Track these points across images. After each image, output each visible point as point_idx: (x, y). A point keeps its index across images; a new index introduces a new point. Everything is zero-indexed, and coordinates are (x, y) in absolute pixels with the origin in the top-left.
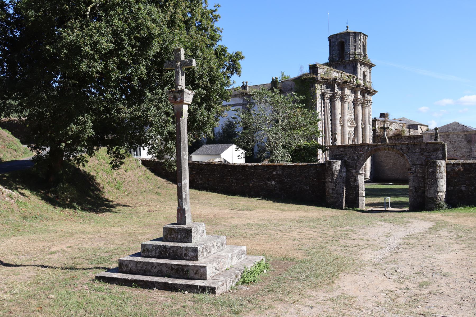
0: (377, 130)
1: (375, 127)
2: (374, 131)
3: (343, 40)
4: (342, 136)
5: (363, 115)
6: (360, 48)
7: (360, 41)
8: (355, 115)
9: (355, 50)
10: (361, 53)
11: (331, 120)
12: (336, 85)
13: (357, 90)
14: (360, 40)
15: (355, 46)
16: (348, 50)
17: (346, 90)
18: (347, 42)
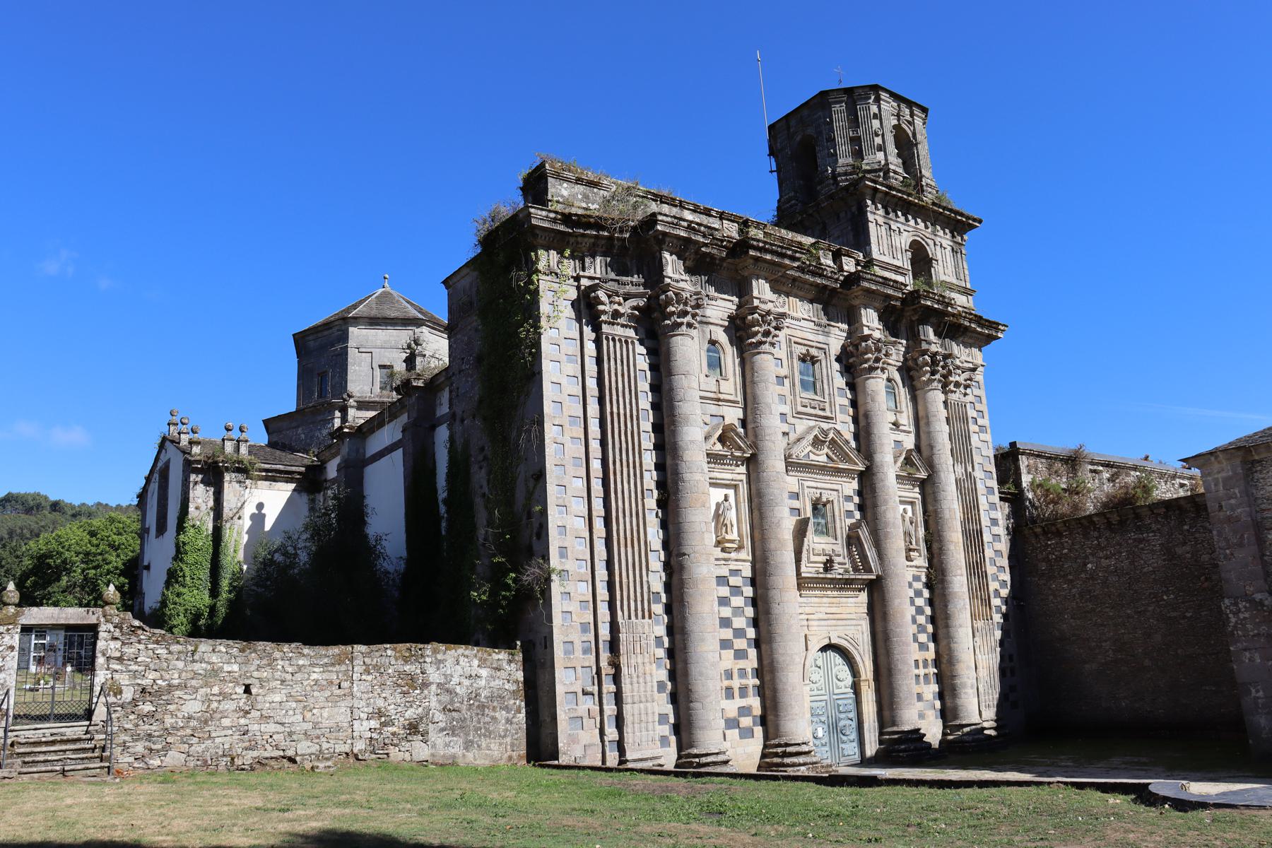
0: (1030, 495)
1: (1018, 483)
2: (1014, 498)
3: (810, 131)
4: (756, 513)
5: (922, 423)
6: (881, 148)
7: (876, 123)
8: (861, 418)
9: (859, 155)
10: (887, 164)
11: (658, 428)
12: (666, 255)
13: (856, 302)
14: (875, 116)
15: (856, 141)
16: (829, 160)
17: (761, 290)
18: (821, 133)
